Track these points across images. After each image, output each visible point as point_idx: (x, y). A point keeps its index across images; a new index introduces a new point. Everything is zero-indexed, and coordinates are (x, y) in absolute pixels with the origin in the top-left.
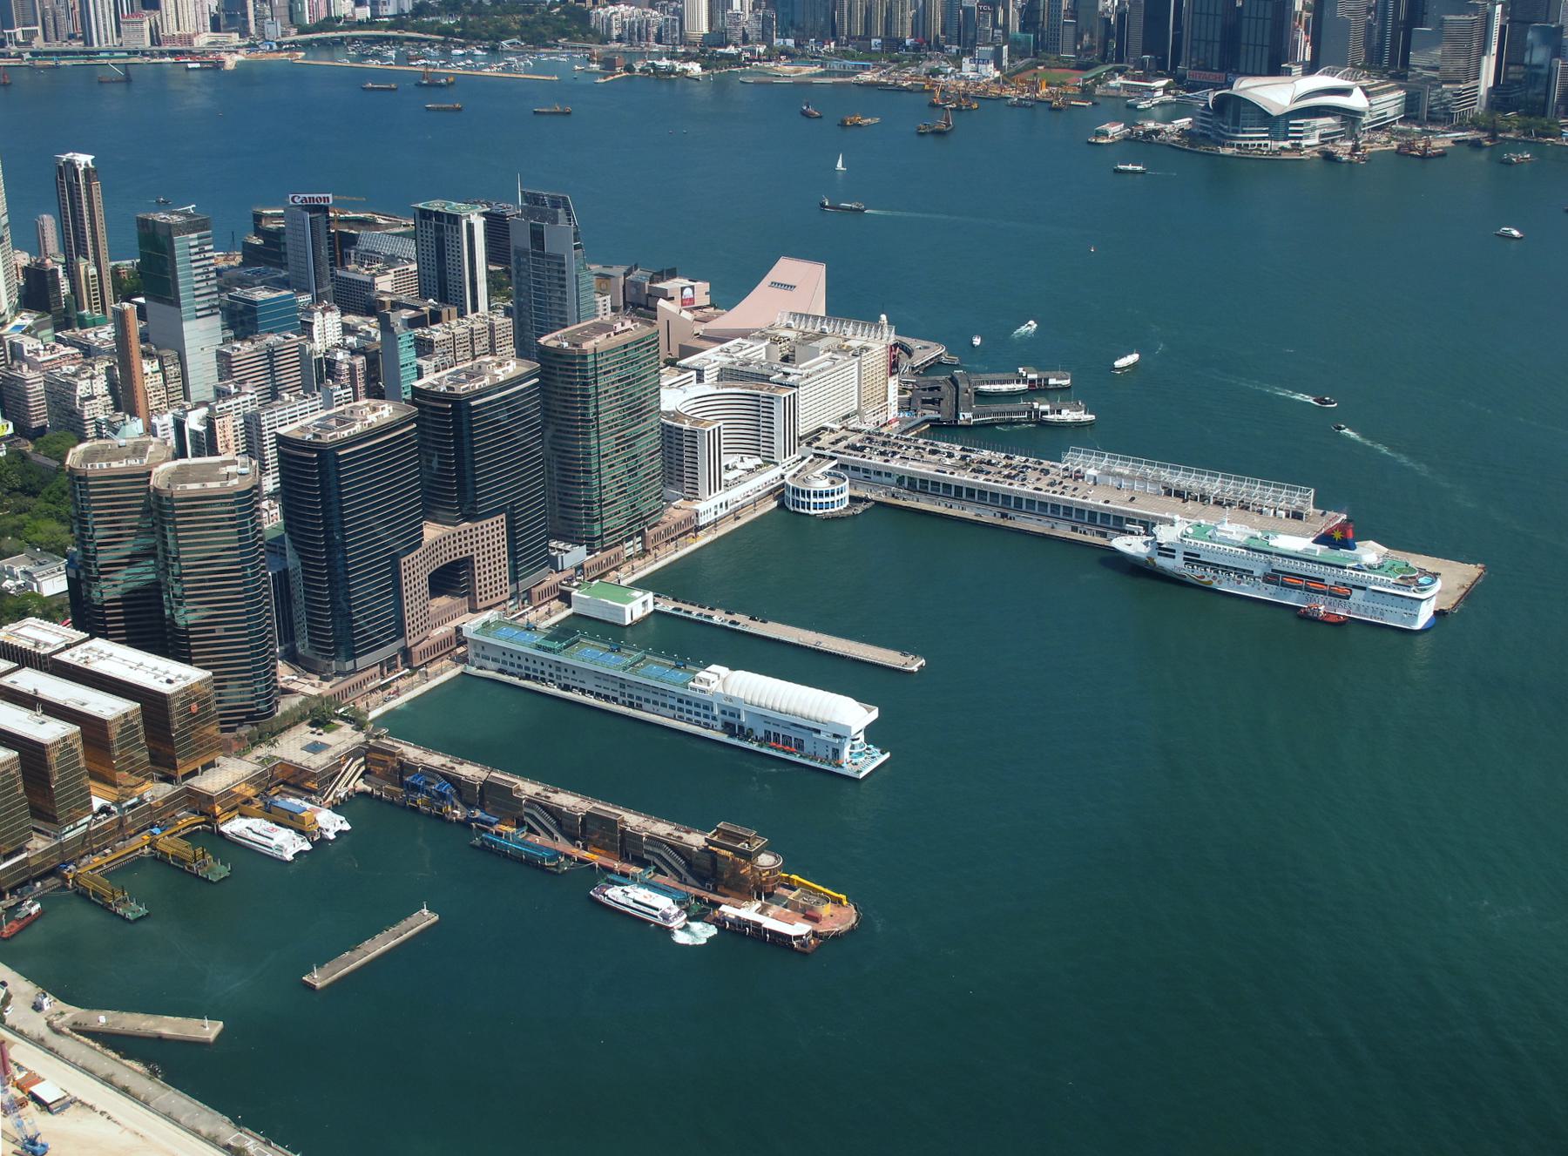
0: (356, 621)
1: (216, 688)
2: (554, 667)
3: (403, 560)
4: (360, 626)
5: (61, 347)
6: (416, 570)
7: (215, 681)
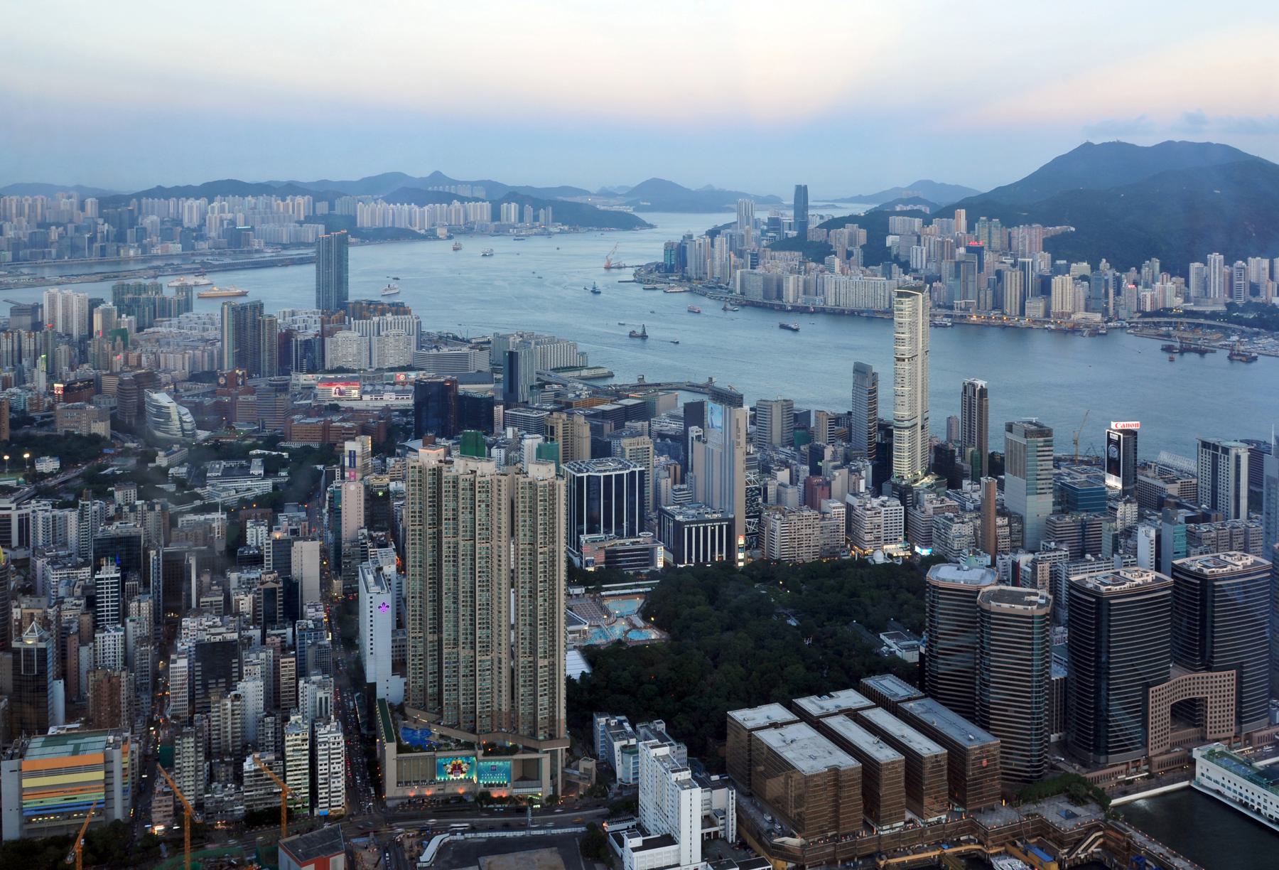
0: (1111, 727)
1: (1002, 752)
2: (1262, 797)
3: (1154, 689)
4: (1114, 731)
5: (947, 499)
6: (1161, 700)
7: (1002, 747)
